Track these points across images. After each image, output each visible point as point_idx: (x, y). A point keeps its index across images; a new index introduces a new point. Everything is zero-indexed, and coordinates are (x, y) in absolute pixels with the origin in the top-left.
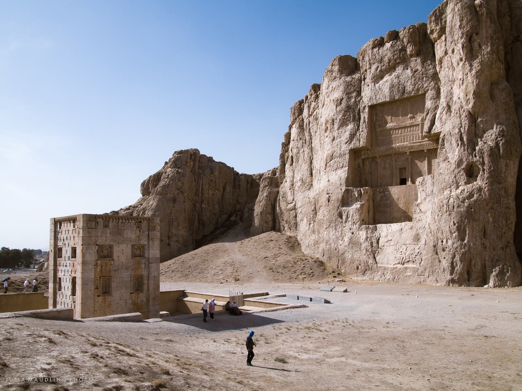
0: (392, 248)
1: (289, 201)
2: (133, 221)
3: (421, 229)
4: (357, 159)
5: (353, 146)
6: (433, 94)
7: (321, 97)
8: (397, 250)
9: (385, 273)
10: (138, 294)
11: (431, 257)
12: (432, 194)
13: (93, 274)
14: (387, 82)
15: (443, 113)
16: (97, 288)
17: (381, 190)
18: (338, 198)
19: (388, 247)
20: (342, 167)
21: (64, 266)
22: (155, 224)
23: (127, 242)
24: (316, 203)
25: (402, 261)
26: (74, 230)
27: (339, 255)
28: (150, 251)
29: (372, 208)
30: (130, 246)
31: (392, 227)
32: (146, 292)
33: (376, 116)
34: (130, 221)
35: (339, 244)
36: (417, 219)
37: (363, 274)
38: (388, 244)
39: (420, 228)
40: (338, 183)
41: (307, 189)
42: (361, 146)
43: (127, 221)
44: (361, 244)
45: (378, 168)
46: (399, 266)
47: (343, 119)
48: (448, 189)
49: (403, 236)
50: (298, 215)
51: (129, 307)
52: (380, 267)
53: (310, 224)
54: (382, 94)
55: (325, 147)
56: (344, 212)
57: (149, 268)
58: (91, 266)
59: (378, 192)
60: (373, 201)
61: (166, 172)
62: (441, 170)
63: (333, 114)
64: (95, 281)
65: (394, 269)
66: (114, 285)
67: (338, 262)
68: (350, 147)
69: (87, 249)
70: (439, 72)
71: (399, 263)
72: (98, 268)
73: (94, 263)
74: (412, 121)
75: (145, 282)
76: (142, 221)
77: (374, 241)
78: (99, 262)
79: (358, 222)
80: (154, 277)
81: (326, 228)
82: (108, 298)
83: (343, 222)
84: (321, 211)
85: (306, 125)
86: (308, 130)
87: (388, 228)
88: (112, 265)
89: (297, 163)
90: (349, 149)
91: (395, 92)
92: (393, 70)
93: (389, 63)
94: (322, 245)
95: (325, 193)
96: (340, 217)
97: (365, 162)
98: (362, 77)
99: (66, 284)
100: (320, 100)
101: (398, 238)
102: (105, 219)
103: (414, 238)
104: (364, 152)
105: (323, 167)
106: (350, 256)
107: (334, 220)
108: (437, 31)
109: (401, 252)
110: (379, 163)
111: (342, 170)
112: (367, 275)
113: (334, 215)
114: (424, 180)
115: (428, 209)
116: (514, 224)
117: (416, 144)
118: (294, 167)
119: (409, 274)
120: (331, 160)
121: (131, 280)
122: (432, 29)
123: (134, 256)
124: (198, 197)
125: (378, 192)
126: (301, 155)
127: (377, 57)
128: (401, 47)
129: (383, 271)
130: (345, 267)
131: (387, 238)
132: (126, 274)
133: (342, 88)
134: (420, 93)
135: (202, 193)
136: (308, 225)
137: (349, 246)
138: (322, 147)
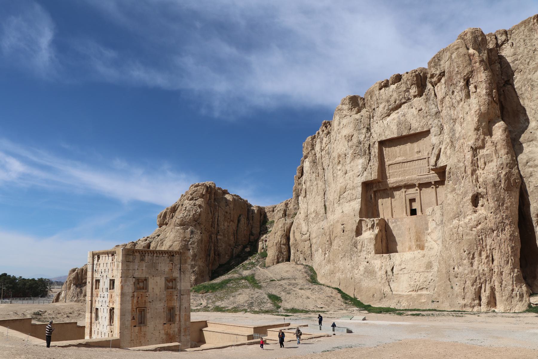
1: (303, 232)
2: (167, 255)
5: (365, 180)
6: (437, 131)
7: (333, 133)
9: (400, 300)
10: (170, 324)
13: (131, 305)
14: (395, 119)
15: (448, 148)
16: (133, 318)
17: (393, 221)
18: (352, 228)
21: (102, 298)
22: (186, 258)
23: (161, 275)
24: (331, 233)
26: (113, 263)
28: (182, 283)
29: (384, 237)
30: (163, 279)
32: (178, 323)
34: (164, 255)
37: (379, 302)
38: (402, 272)
40: (352, 214)
41: (321, 220)
42: (372, 179)
43: (161, 255)
46: (414, 293)
47: (355, 153)
48: (457, 218)
50: (313, 245)
51: (162, 337)
53: (325, 254)
54: (390, 131)
55: (338, 179)
57: (180, 300)
58: (129, 298)
59: (390, 222)
60: (386, 231)
61: (182, 205)
62: (449, 201)
63: (345, 149)
64: (132, 312)
66: (148, 316)
68: (362, 179)
69: (126, 281)
71: (414, 290)
72: (135, 299)
73: (131, 295)
74: (418, 156)
75: (177, 313)
76: (175, 255)
77: (389, 269)
78: (135, 293)
80: (185, 308)
82: (143, 329)
83: (358, 252)
84: (336, 242)
85: (319, 159)
86: (320, 164)
87: (402, 257)
88: (147, 297)
89: (310, 195)
90: (362, 182)
91: (402, 129)
93: (395, 102)
94: (337, 274)
95: (339, 224)
97: (377, 194)
98: (371, 115)
99: (104, 315)
100: (332, 136)
102: (141, 253)
103: (427, 265)
105: (336, 199)
107: (349, 249)
108: (437, 75)
111: (355, 202)
112: (383, 303)
113: (350, 245)
114: (433, 210)
116: (519, 250)
118: (307, 199)
119: (423, 301)
121: (164, 312)
122: (432, 73)
123: (167, 288)
124: (214, 228)
125: (390, 222)
126: (314, 187)
127: (384, 98)
128: (405, 88)
132: (159, 305)
133: (352, 125)
134: (425, 130)
135: (218, 224)
136: (324, 255)
137: (365, 275)
138: (335, 180)
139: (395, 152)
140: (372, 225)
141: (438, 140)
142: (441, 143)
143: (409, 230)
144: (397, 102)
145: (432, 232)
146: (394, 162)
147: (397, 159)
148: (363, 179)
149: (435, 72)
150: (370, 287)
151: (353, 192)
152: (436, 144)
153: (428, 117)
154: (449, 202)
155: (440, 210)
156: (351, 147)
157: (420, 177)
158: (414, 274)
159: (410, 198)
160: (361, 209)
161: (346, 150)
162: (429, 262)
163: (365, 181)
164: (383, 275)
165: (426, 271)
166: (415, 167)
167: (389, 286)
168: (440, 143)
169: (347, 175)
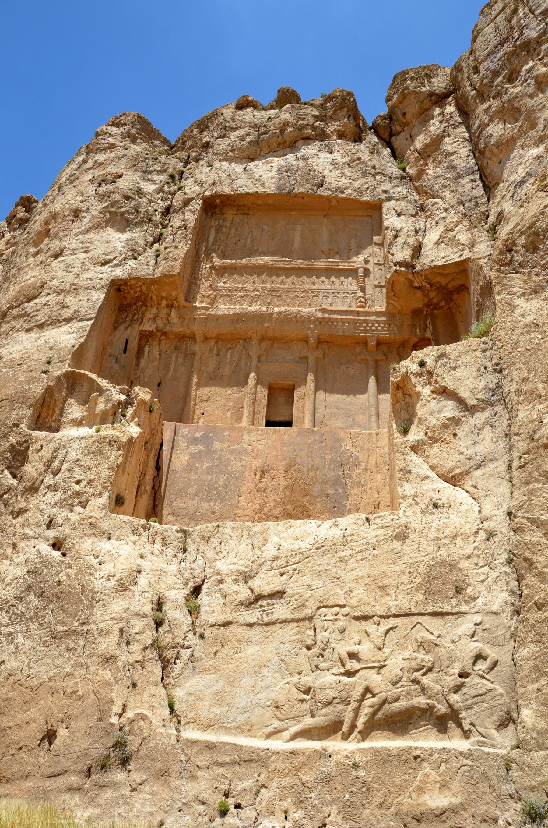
4: (122, 328)
8: (316, 650)
12: (495, 398)
17: (198, 435)
20: (68, 320)
25: (357, 712)
33: (217, 231)
39: (454, 537)
42: (156, 276)
44: (93, 601)
47: (111, 213)
56: (38, 446)
68: (114, 273)
79: (100, 495)
90: (112, 277)
91: (295, 179)
92: (288, 150)
97: (147, 349)
103: (429, 578)
104: (154, 310)
110: (197, 358)
111: (66, 328)
120: (30, 300)
134: (366, 198)
139: (249, 242)
141: (410, 223)
142: (420, 233)
143: (261, 478)
144: (290, 129)
145: (434, 440)
148: (119, 273)
149: (416, 88)
150: (34, 682)
151: (69, 300)
152: (406, 229)
154: (530, 318)
156: (101, 197)
157: (327, 316)
158: (340, 624)
160: (82, 345)
161: (82, 202)
162: (442, 563)
163: (126, 275)
165: (430, 610)
166: (314, 287)
168: (417, 232)
169: (62, 258)
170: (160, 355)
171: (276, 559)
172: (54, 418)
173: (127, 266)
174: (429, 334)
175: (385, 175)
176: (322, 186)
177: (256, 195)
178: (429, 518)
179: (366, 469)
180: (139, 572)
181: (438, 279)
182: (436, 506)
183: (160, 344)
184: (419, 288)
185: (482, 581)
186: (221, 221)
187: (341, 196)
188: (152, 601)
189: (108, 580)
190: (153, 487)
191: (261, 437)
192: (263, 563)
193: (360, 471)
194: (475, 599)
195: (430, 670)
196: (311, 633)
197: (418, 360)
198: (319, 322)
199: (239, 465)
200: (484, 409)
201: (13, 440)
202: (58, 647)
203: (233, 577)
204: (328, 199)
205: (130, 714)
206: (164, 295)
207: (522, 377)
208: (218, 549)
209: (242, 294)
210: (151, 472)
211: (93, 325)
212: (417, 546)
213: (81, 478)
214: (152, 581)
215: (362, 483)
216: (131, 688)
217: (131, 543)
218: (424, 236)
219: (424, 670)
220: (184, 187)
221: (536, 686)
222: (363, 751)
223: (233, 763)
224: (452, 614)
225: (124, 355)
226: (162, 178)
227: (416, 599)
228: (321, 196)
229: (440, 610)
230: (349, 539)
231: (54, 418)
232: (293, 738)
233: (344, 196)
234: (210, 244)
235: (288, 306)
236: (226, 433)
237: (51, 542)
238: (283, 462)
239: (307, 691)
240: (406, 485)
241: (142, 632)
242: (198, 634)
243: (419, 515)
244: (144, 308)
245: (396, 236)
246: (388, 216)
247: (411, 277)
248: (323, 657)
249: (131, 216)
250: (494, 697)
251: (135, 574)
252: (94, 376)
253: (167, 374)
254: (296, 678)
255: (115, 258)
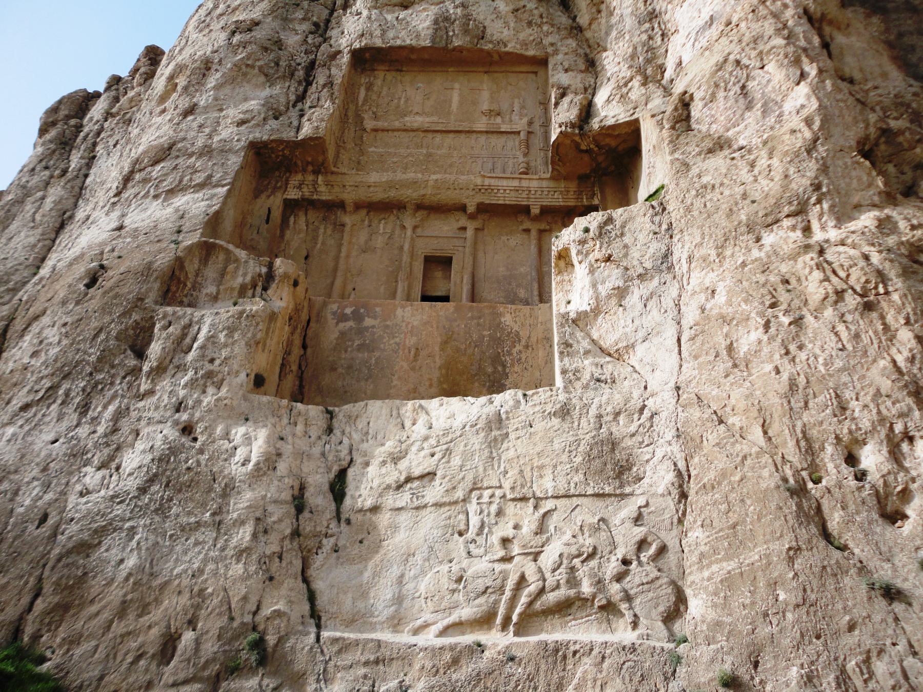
0: (430, 521)
3: (622, 419)
4: (263, 196)
8: (470, 535)
11: (791, 560)
17: (348, 311)
19: (404, 519)
27: (57, 551)
31: (433, 414)
35: (78, 488)
36: (586, 376)
39: (617, 414)
45: (341, 245)
47: (247, 66)
49: (511, 453)
52: (345, 647)
59: (334, 313)
60: (304, 347)
65: (455, 661)
67: (25, 600)
70: (590, 24)
81: (25, 407)
83: (146, 368)
91: (453, 31)
96: (133, 348)
97: (292, 219)
101: (478, 461)
103: (589, 458)
104: (299, 177)
106: (132, 562)
109: (505, 541)
110: (347, 228)
111: (200, 195)
113: (102, 336)
115: (641, 334)
117: (505, 183)
129: (362, 671)
130: (73, 641)
131: (403, 465)
134: (531, 53)
140: (260, 275)
142: (590, 91)
143: (417, 355)
146: (397, 124)
147: (407, 119)
153: (545, 28)
154: (705, 180)
155: (647, 219)
157: (487, 182)
158: (494, 508)
159: (429, 251)
160: (217, 214)
164: (270, 508)
165: (590, 491)
167: (306, 580)
170: (307, 226)
171: (426, 439)
172: (185, 292)
173: (268, 127)
174: (596, 202)
175: (552, 26)
176: (483, 38)
177: (411, 49)
178: (591, 394)
179: (527, 347)
180: (279, 455)
181: (608, 140)
182: (598, 380)
183: (306, 215)
184: (586, 151)
185: (647, 461)
186: (372, 79)
187: (503, 50)
188: (292, 487)
189: (243, 465)
190: (300, 367)
191: (415, 312)
192: (412, 444)
193: (521, 348)
194: (640, 479)
195: (591, 556)
196: (462, 517)
197: (582, 227)
198: (479, 190)
199: (392, 342)
200: (652, 277)
201: (135, 316)
202: (186, 540)
203: (381, 459)
204: (489, 53)
205: (266, 611)
206: (310, 159)
207: (694, 244)
208: (365, 430)
209: (395, 160)
210: (297, 351)
211: (229, 191)
212: (576, 424)
213: (216, 356)
214: (293, 466)
215: (523, 359)
216: (267, 582)
217: (270, 425)
218: (593, 95)
219: (585, 555)
220: (330, 38)
221: (706, 574)
222: (518, 645)
223: (377, 662)
224: (616, 495)
225: (266, 226)
226: (306, 27)
227: (576, 479)
228: (482, 50)
229: (601, 492)
230: (504, 416)
231: (185, 292)
232: (443, 633)
233: (507, 49)
234: (360, 103)
235: (445, 172)
236: (378, 309)
237: (181, 426)
238: (439, 340)
239: (459, 580)
240: (566, 359)
241: (280, 521)
242: (343, 520)
243: (580, 391)
244: (288, 175)
245: (563, 95)
246: (554, 72)
247: (577, 139)
248: (476, 542)
249: (271, 71)
250: (661, 586)
251: (274, 458)
252: (231, 247)
253: (315, 247)
254: (445, 568)
255: (253, 118)
